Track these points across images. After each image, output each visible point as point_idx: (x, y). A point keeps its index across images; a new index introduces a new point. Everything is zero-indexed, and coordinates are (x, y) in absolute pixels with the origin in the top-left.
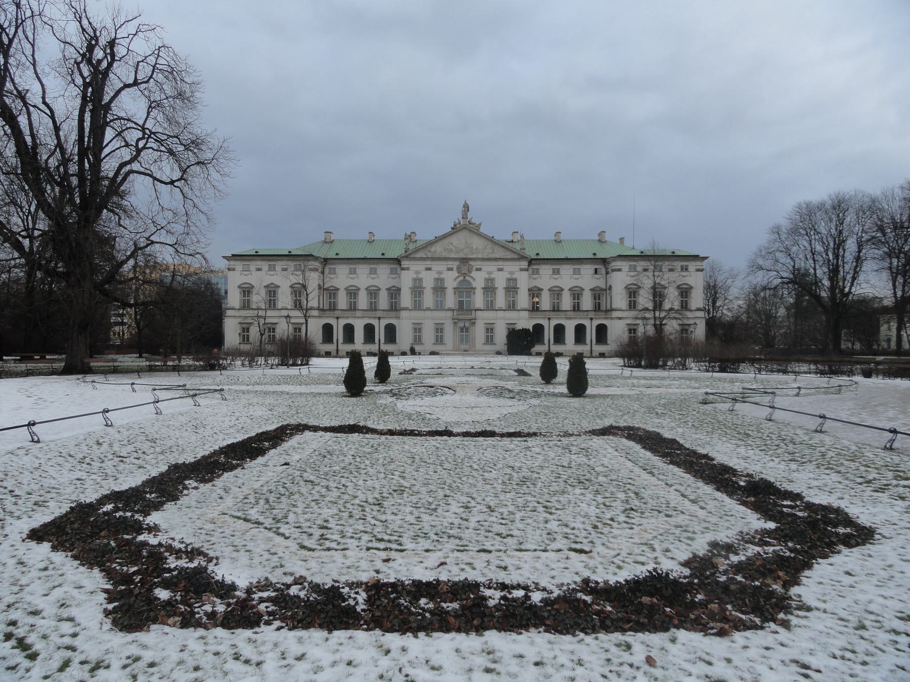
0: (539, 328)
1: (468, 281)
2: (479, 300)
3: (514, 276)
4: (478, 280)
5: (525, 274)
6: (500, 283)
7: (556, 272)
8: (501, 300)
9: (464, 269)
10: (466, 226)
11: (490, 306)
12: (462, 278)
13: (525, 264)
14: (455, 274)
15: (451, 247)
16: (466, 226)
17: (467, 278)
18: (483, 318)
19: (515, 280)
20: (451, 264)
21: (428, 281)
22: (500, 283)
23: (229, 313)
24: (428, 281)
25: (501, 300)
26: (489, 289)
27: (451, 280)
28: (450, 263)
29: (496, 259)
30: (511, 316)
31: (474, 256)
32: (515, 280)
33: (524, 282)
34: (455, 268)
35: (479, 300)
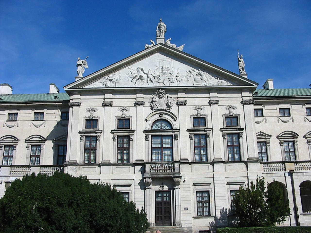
0: (277, 189)
2: (184, 147)
3: (234, 112)
5: (250, 108)
8: (218, 146)
9: (161, 102)
11: (202, 156)
12: (157, 117)
14: (145, 111)
15: (142, 73)
17: (165, 117)
18: (190, 175)
19: (236, 118)
21: (108, 123)
24: (108, 123)
25: (218, 146)
27: (142, 119)
29: (208, 90)
30: (237, 172)
31: (175, 84)
32: (236, 118)
34: (147, 103)
35: (184, 147)
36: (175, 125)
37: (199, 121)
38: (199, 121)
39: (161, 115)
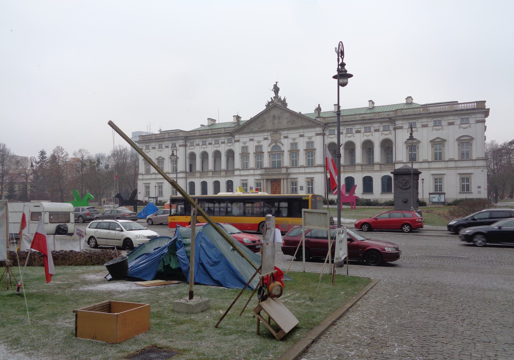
1: (278, 146)
4: (286, 146)
6: (302, 146)
7: (342, 133)
10: (277, 105)
11: (294, 164)
12: (274, 144)
13: (319, 130)
16: (277, 105)
17: (278, 144)
20: (266, 135)
22: (302, 146)
23: (140, 177)
26: (294, 152)
28: (266, 134)
33: (318, 143)
36: (283, 148)
37: (294, 145)
38: (294, 145)
39: (276, 143)
